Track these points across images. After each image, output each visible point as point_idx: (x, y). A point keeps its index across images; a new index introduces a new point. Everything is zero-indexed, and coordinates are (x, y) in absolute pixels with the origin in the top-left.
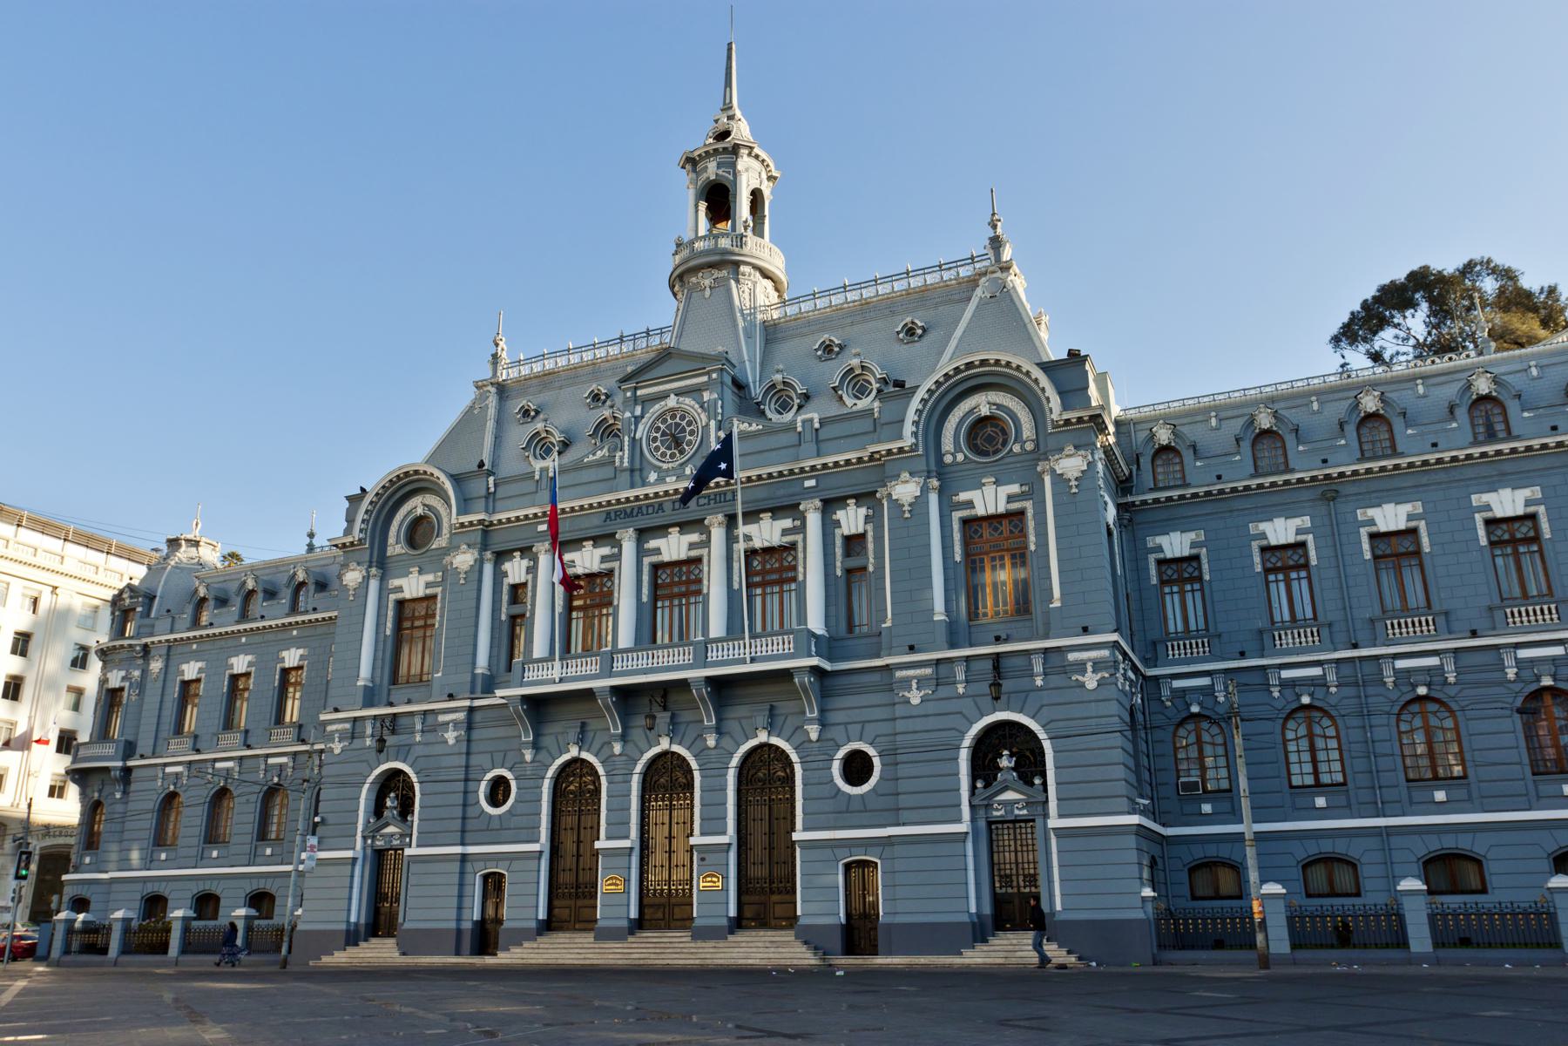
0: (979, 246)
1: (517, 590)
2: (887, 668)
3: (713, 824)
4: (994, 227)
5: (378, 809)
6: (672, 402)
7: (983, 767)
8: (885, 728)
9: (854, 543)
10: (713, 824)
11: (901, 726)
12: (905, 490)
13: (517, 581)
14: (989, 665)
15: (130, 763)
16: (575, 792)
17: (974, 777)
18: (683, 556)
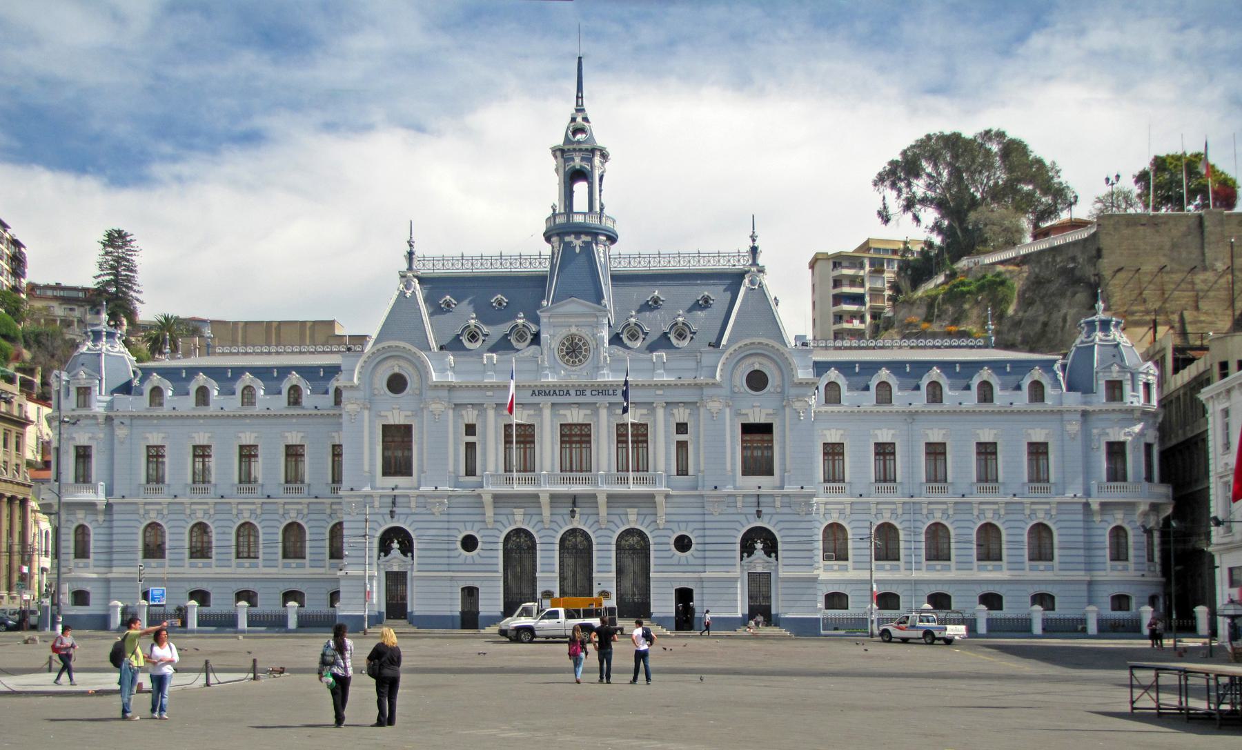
0: (746, 246)
1: (470, 430)
2: (702, 496)
3: (604, 568)
4: (754, 240)
5: (385, 548)
6: (573, 330)
7: (747, 547)
8: (700, 525)
9: (682, 428)
10: (604, 568)
11: (708, 525)
12: (714, 406)
13: (470, 422)
14: (755, 499)
15: (111, 501)
16: (519, 548)
17: (742, 553)
18: (581, 421)
